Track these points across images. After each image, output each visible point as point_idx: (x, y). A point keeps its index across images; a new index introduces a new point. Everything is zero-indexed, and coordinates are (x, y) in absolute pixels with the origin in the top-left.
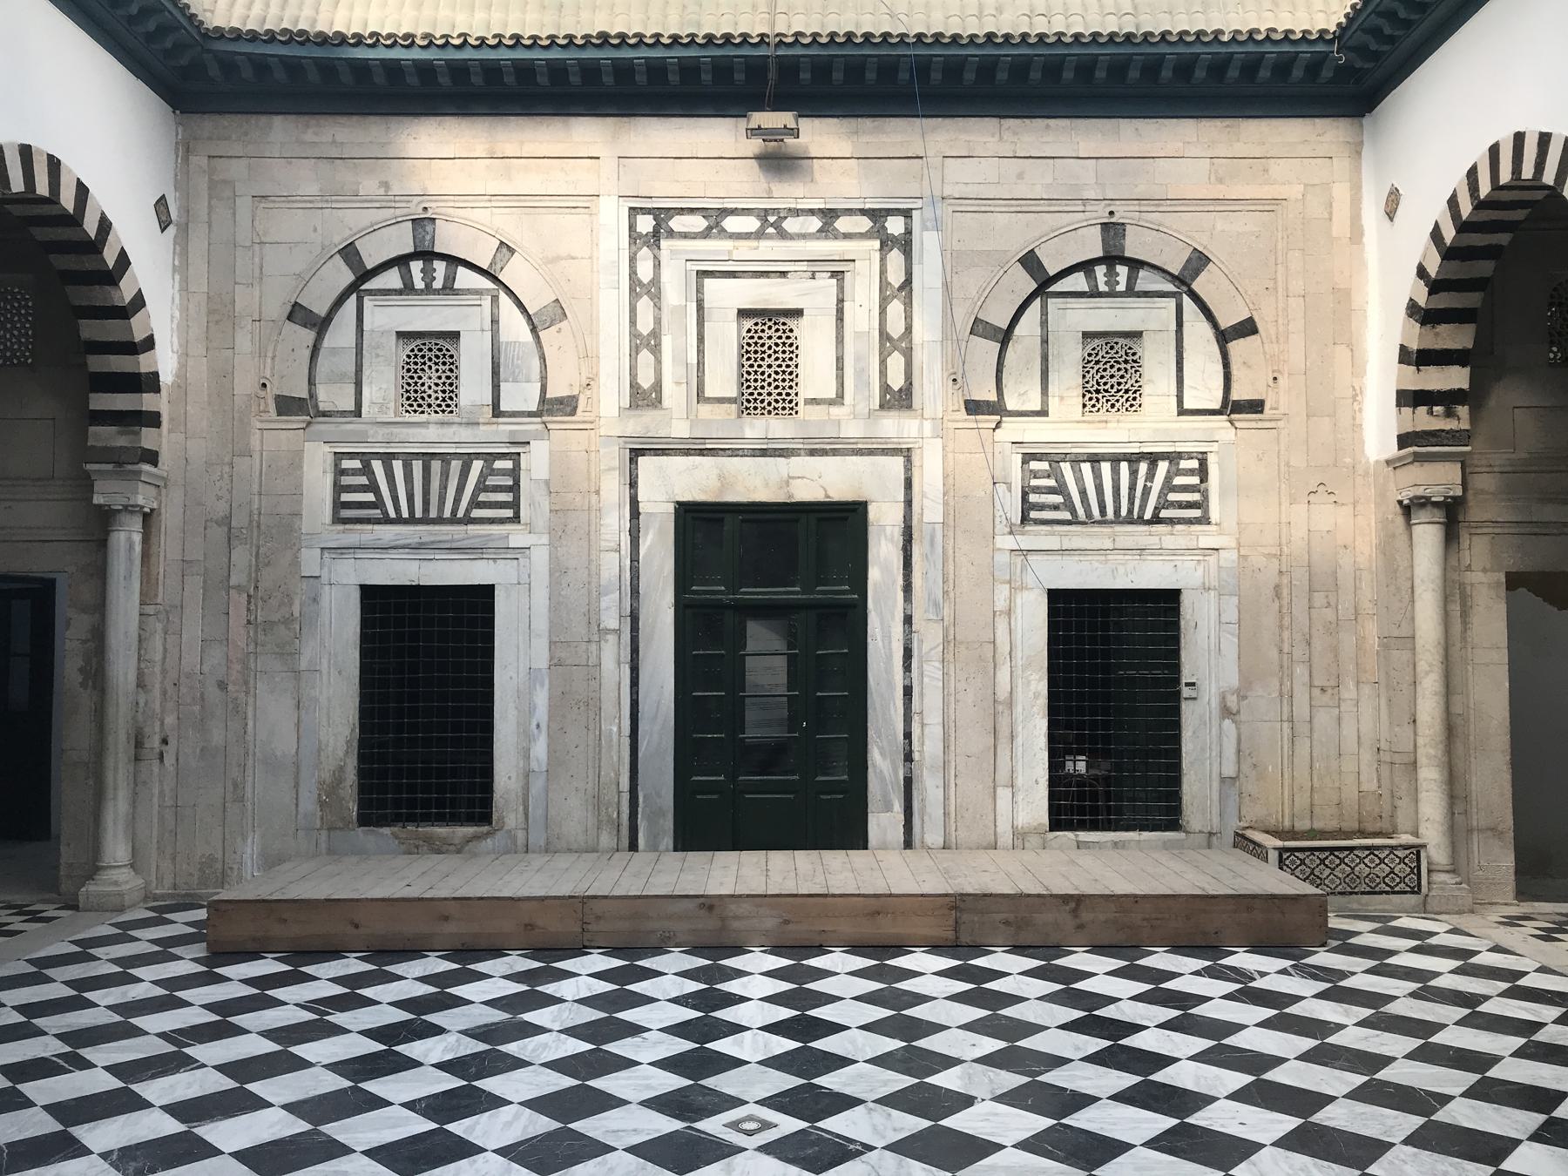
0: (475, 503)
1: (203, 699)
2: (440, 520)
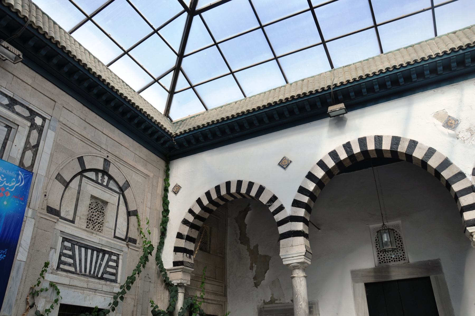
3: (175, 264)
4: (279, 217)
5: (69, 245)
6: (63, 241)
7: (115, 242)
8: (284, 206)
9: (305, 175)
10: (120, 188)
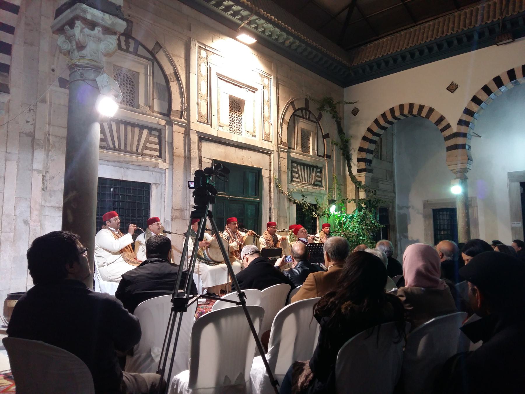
1: (15, 229)
2: (130, 152)
5: (295, 165)
6: (292, 163)
8: (451, 124)
10: (316, 119)
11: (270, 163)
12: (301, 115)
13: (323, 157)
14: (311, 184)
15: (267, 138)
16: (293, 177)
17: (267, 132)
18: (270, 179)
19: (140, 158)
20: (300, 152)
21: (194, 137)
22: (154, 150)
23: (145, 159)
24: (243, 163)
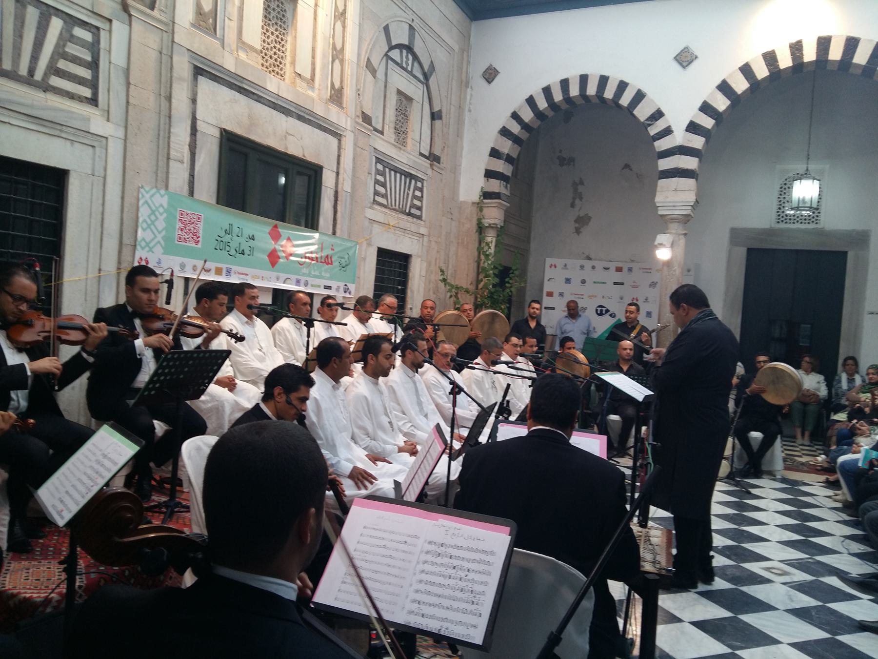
0: (53, 70)
3: (486, 195)
4: (662, 145)
5: (380, 167)
7: (420, 161)
8: (673, 128)
9: (716, 85)
11: (339, 156)
12: (398, 60)
13: (427, 158)
14: (403, 212)
15: (337, 96)
16: (376, 193)
17: (337, 85)
18: (336, 192)
19: (38, 97)
20: (392, 141)
21: (182, 67)
22: (80, 81)
23: (54, 100)
24: (287, 148)
